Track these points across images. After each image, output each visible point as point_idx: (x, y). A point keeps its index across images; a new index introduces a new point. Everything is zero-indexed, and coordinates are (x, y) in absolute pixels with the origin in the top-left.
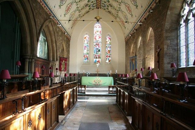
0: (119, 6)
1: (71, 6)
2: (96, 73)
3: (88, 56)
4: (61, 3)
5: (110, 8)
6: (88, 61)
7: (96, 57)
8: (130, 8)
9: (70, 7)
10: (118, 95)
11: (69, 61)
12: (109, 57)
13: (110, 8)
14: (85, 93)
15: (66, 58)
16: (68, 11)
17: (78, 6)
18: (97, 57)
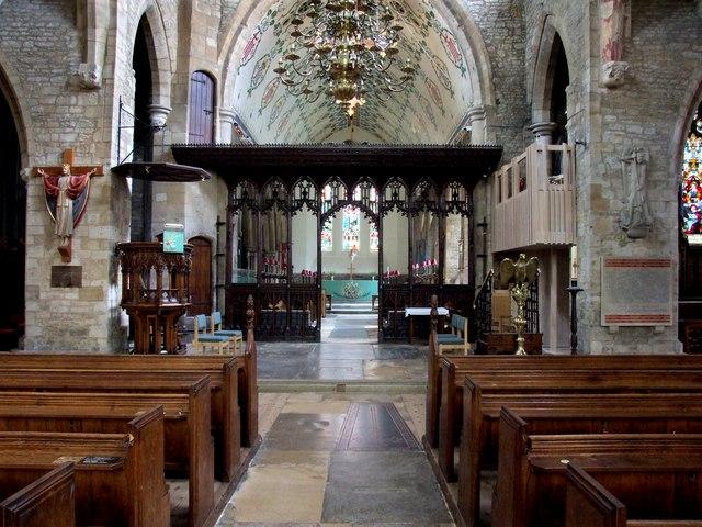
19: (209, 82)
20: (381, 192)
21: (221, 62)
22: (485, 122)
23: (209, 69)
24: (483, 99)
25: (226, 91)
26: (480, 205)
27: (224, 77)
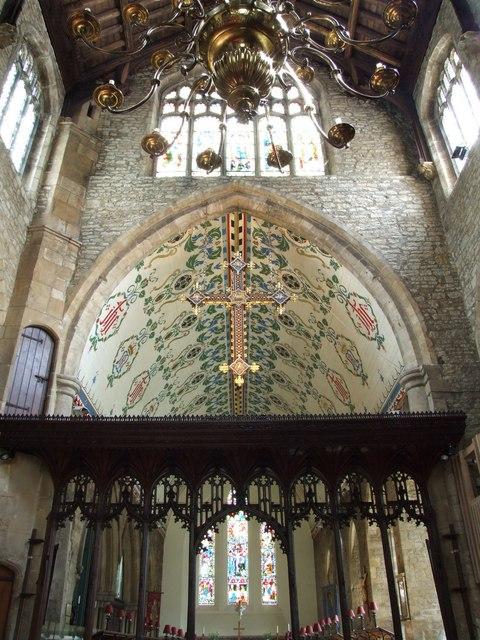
0: (307, 380)
1: (147, 380)
4: (115, 371)
5: (276, 387)
8: (343, 385)
9: (144, 386)
13: (276, 387)
16: (138, 399)
17: (170, 381)
19: (48, 342)
20: (287, 491)
21: (68, 319)
22: (428, 388)
23: (50, 324)
24: (419, 359)
25: (70, 355)
26: (440, 505)
27: (70, 337)
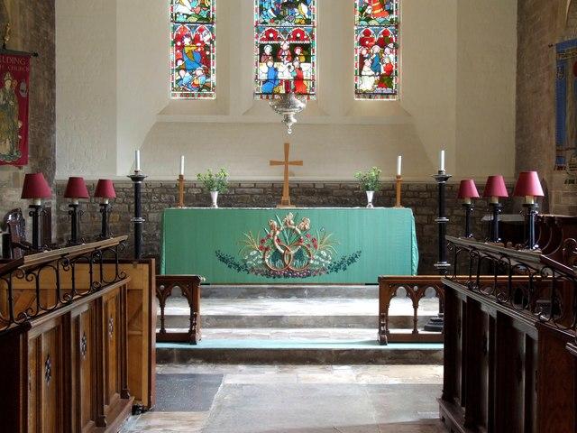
2: (272, 175)
3: (206, 38)
6: (213, 78)
7: (276, 49)
10: (468, 347)
11: (52, 84)
12: (383, 43)
14: (190, 338)
15: (25, 58)
18: (285, 46)
